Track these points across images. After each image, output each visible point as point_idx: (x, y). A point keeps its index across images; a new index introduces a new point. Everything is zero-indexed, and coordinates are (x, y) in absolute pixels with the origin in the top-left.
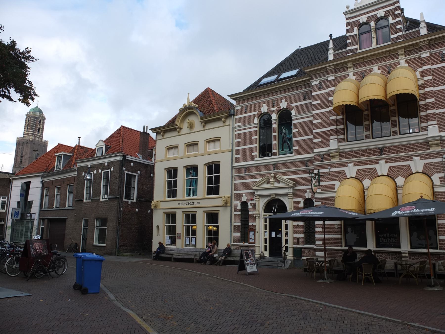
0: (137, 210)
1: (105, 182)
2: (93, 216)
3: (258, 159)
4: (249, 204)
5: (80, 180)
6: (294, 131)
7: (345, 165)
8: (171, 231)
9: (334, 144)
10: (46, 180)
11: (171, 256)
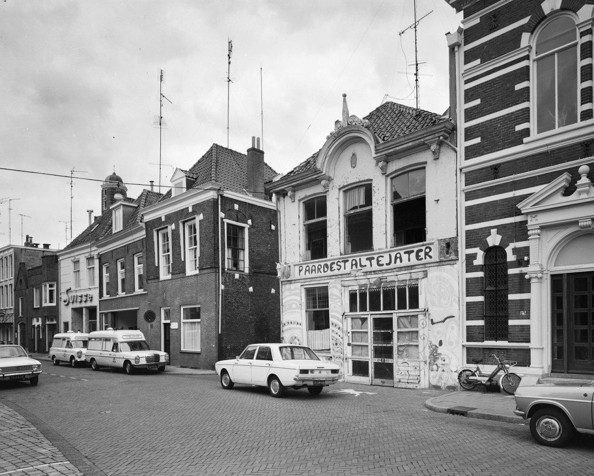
0: (251, 289)
2: (177, 303)
4: (509, 250)
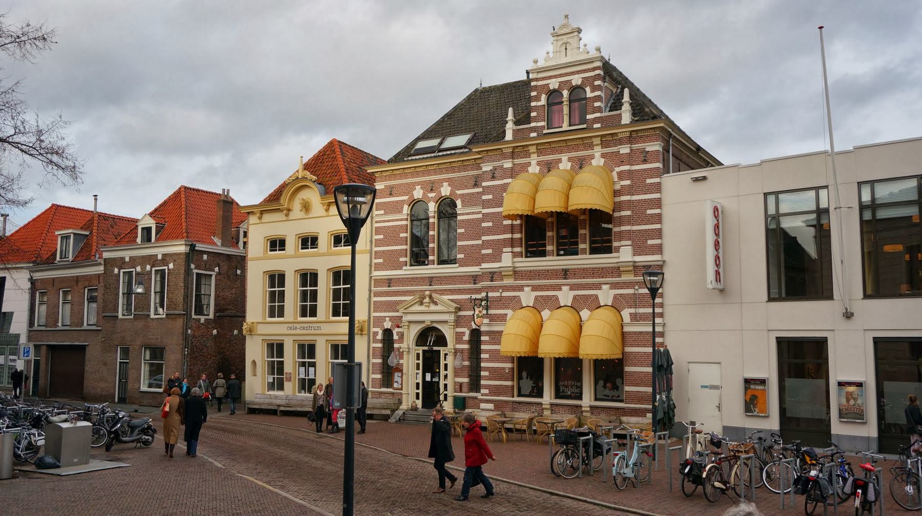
0: (215, 332)
1: (159, 283)
3: (408, 267)
4: (394, 332)
5: (108, 281)
6: (459, 231)
7: (520, 288)
8: (277, 368)
9: (507, 260)
10: (37, 276)
11: (276, 408)
